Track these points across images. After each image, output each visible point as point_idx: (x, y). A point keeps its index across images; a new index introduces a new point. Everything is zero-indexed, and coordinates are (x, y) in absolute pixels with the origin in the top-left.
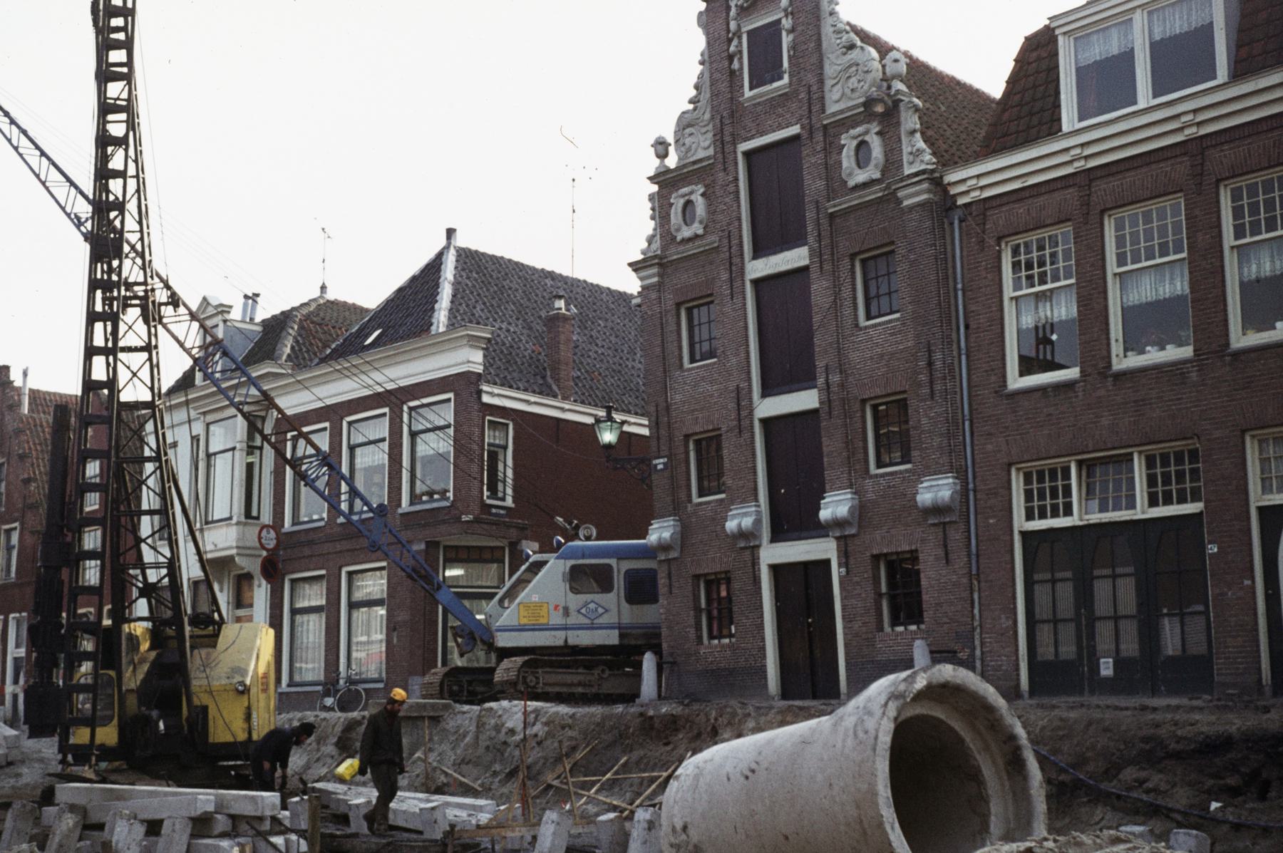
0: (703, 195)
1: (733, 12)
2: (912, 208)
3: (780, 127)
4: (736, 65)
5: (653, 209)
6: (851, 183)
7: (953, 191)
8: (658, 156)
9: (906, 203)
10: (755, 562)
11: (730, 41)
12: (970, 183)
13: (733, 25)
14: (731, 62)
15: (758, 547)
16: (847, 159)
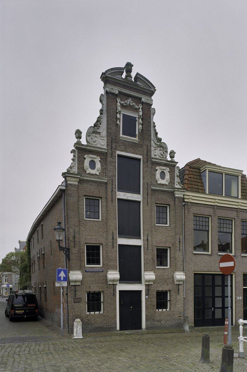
0: (100, 161)
1: (118, 104)
2: (178, 197)
3: (133, 153)
4: (118, 122)
5: (74, 156)
6: (159, 182)
7: (185, 197)
8: (77, 138)
9: (176, 195)
10: (114, 290)
11: (117, 113)
12: (190, 197)
13: (119, 108)
14: (117, 121)
15: (116, 284)
16: (158, 175)
